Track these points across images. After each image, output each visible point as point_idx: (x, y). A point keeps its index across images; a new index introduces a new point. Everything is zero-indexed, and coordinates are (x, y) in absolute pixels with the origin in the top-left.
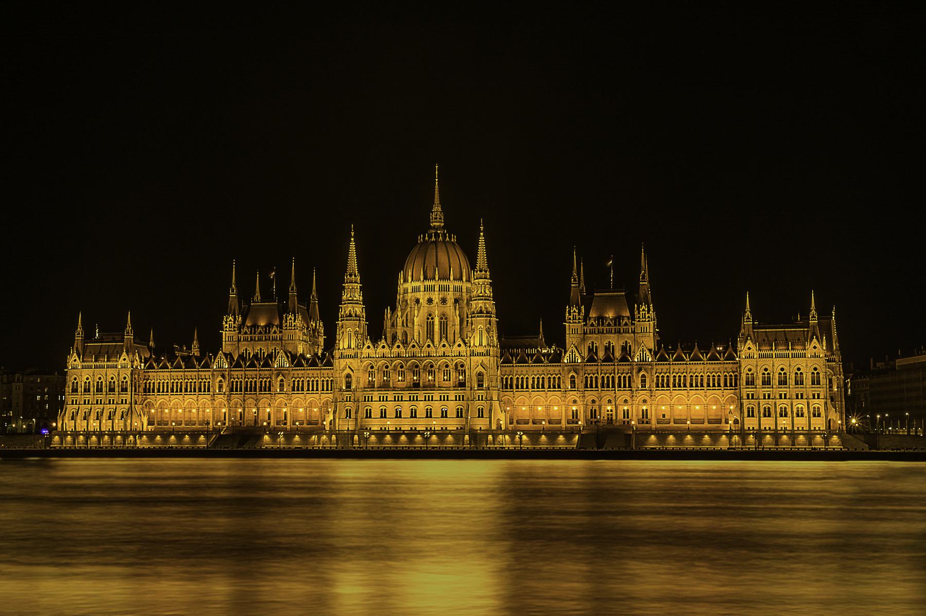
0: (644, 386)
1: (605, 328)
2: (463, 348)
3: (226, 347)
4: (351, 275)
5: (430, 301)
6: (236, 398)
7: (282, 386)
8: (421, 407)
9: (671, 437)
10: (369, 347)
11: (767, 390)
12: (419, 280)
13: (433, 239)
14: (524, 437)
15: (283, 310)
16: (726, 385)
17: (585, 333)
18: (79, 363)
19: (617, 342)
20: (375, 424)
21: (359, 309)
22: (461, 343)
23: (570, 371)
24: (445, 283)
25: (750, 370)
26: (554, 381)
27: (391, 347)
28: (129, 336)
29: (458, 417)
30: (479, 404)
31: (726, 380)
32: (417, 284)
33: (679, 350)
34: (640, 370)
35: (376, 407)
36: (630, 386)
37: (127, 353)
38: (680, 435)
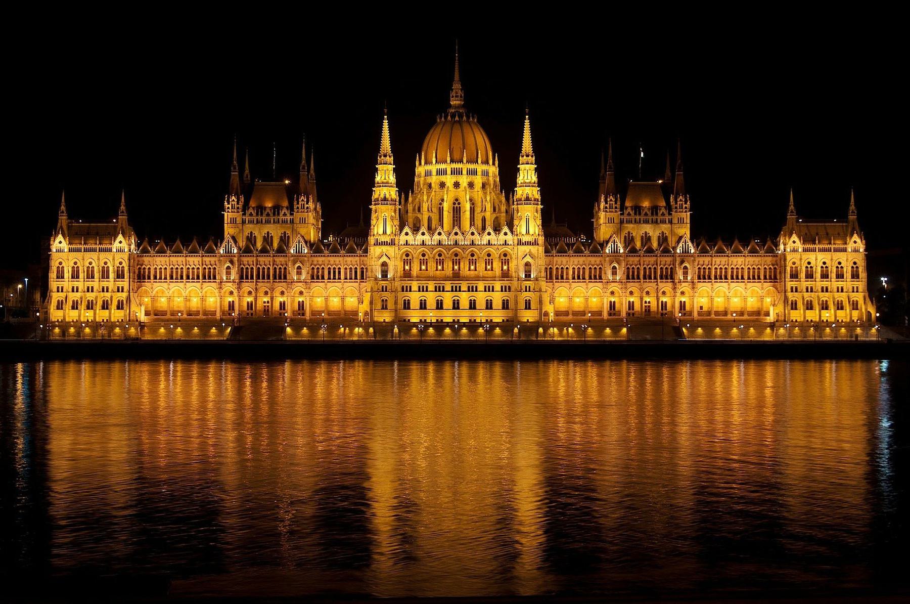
0: (685, 277)
1: (642, 218)
2: (509, 237)
3: (228, 230)
4: (385, 156)
5: (457, 185)
6: (247, 286)
8: (464, 298)
9: (718, 330)
10: (407, 234)
11: (809, 284)
12: (445, 162)
13: (457, 118)
14: (570, 330)
15: (292, 193)
16: (765, 278)
17: (622, 222)
18: (65, 245)
19: (653, 232)
20: (414, 316)
21: (392, 193)
23: (611, 262)
24: (472, 166)
25: (794, 263)
26: (595, 272)
28: (123, 218)
29: (503, 308)
30: (526, 295)
31: (765, 272)
32: (443, 166)
33: (720, 243)
34: (682, 262)
35: (415, 298)
36: (672, 278)
38: (726, 326)
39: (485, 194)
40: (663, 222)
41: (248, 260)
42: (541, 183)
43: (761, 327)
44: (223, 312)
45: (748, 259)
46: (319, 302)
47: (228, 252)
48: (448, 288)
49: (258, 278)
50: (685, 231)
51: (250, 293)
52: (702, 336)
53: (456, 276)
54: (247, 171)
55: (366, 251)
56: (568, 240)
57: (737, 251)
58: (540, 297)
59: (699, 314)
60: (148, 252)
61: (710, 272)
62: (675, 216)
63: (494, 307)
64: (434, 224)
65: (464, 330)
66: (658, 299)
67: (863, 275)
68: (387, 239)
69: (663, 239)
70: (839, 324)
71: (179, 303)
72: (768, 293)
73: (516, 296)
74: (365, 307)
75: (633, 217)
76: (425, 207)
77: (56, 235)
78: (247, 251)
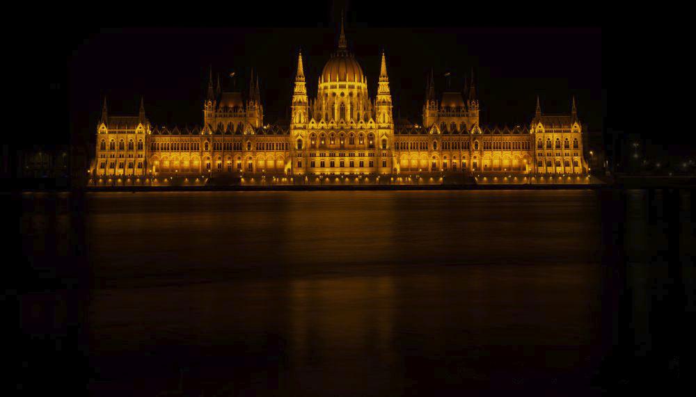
2: (373, 125)
3: (207, 120)
4: (300, 77)
5: (342, 94)
6: (218, 155)
7: (249, 146)
8: (347, 160)
10: (313, 123)
11: (549, 151)
12: (336, 81)
14: (410, 179)
15: (245, 98)
16: (523, 148)
17: (439, 116)
18: (106, 130)
19: (457, 122)
20: (318, 171)
21: (304, 98)
22: (373, 121)
24: (350, 83)
25: (540, 139)
27: (327, 123)
28: (142, 113)
29: (370, 166)
30: (384, 159)
31: (523, 145)
32: (334, 83)
33: (496, 128)
34: (474, 139)
35: (318, 160)
36: (469, 148)
37: (142, 123)
38: (501, 176)
39: (359, 99)
40: (463, 116)
41: (218, 139)
42: (392, 93)
43: (521, 177)
44: (203, 170)
45: (513, 137)
46: (261, 163)
47: (207, 134)
48: (337, 154)
49: (224, 149)
50: (476, 121)
51: (219, 158)
52: (487, 182)
53: (342, 147)
54: (218, 86)
55: (289, 133)
56: (408, 126)
57: (506, 133)
58: (392, 159)
59: (485, 169)
60: (158, 134)
61: (491, 145)
62: (470, 112)
63: (364, 165)
64: (329, 117)
65: (347, 179)
66: (460, 161)
67: (580, 146)
68: (301, 125)
69: (463, 126)
70: (567, 175)
71: (176, 163)
72: (525, 157)
73: (377, 159)
74: (289, 166)
75: (445, 113)
76: (324, 106)
77: (101, 124)
78: (218, 133)
